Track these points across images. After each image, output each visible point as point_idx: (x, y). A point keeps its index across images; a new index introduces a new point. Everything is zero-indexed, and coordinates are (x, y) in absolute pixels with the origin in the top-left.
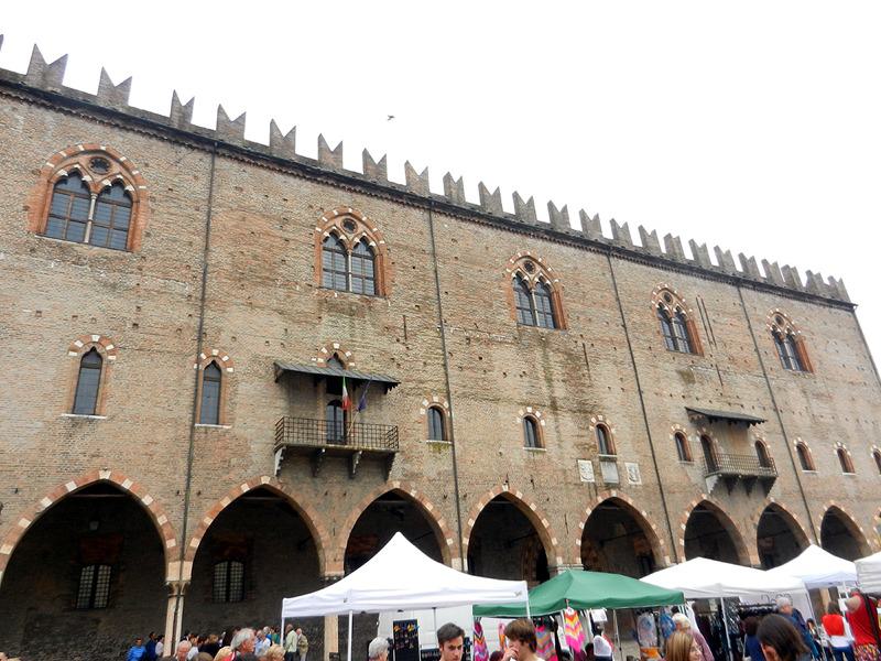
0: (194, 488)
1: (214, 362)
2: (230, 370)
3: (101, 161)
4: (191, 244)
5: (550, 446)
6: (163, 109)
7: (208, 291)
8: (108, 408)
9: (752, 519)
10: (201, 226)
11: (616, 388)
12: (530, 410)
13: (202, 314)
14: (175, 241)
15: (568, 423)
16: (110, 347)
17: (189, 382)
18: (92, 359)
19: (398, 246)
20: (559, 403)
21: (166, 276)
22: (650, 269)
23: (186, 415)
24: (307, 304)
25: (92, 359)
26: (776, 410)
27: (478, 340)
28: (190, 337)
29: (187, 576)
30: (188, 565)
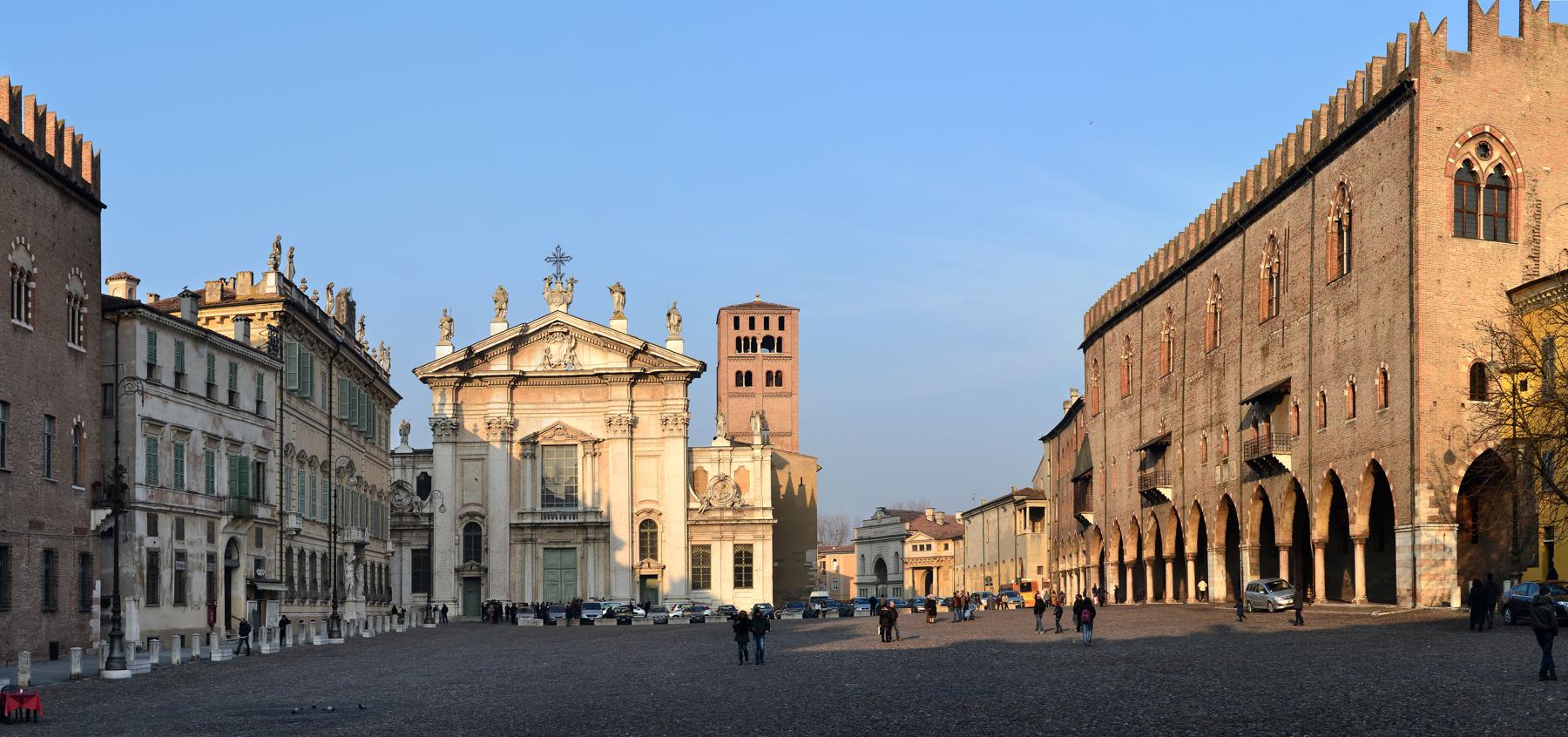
24: (1156, 391)
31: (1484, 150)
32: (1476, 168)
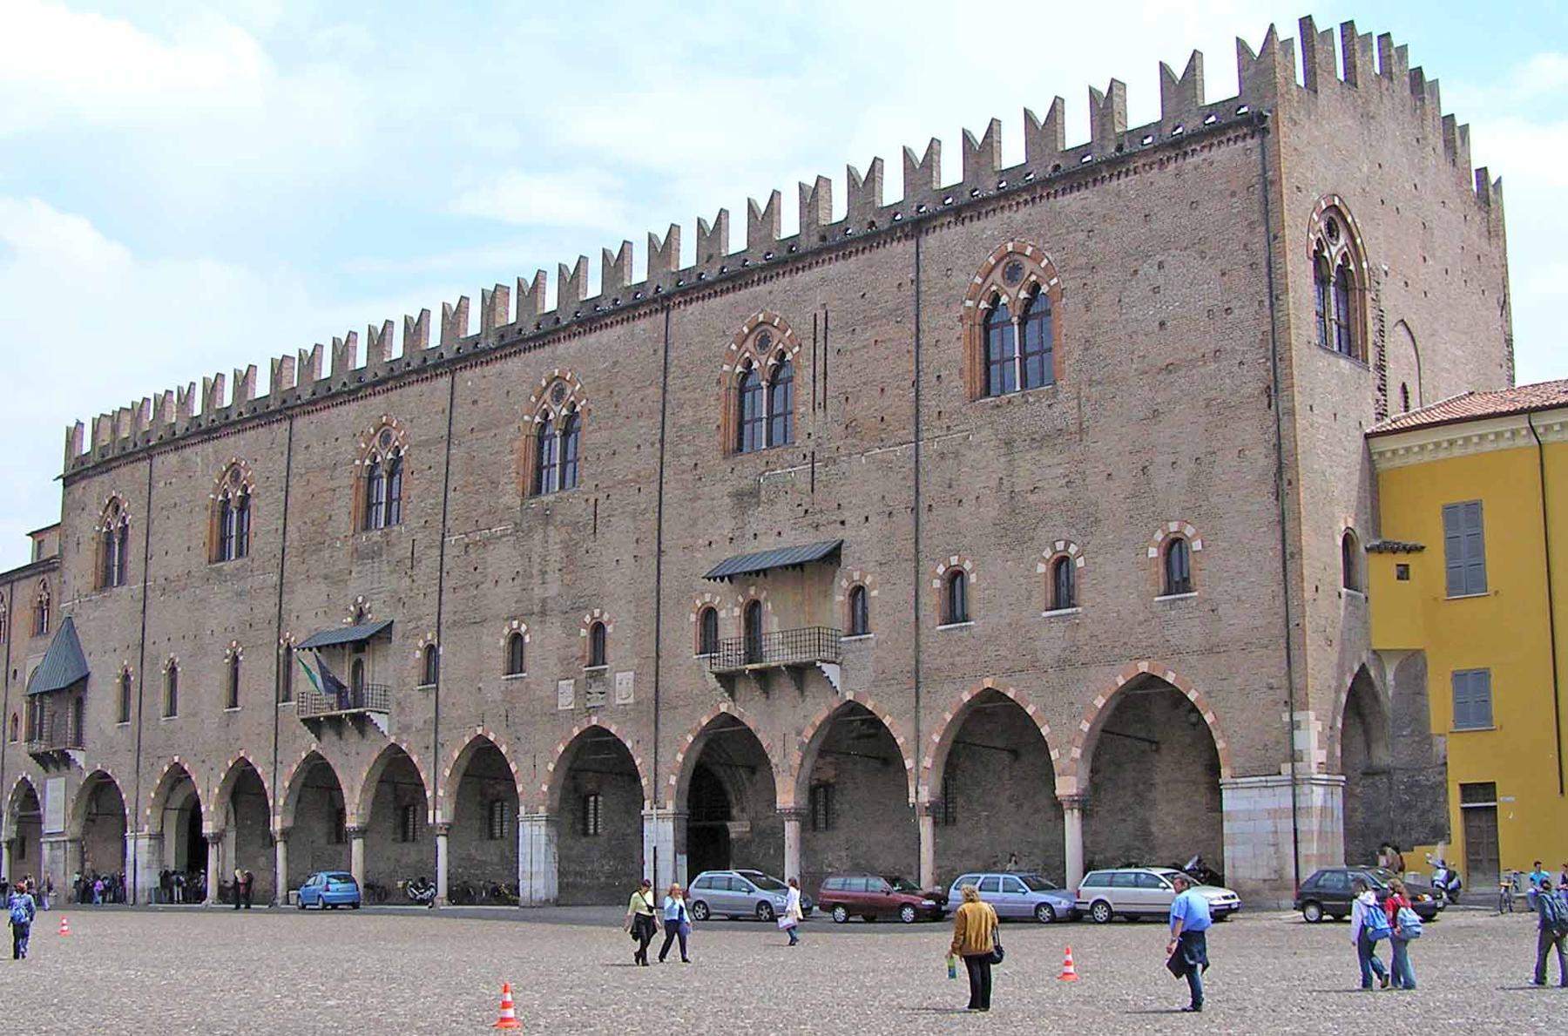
5: (531, 671)
9: (799, 733)
11: (627, 559)
12: (515, 624)
15: (555, 628)
18: (236, 659)
19: (419, 445)
20: (551, 604)
22: (744, 294)
26: (915, 510)
27: (476, 543)
31: (1331, 229)
32: (1326, 254)
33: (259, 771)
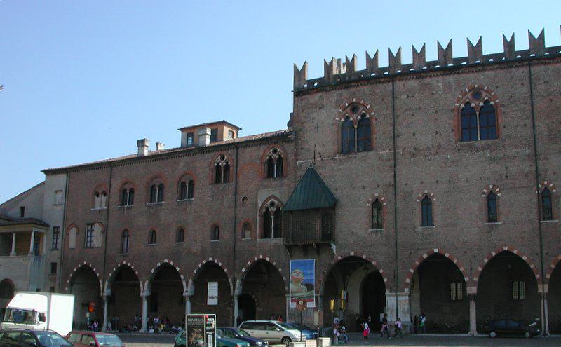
0: (544, 252)
1: (546, 188)
2: (554, 191)
3: (477, 94)
4: (525, 125)
6: (500, 49)
7: (538, 149)
8: (502, 217)
10: (529, 113)
13: (536, 163)
14: (518, 126)
16: (498, 190)
17: (535, 200)
18: (492, 197)
21: (516, 147)
23: (534, 216)
25: (492, 197)
28: (532, 177)
29: (546, 290)
30: (546, 286)
33: (524, 258)
